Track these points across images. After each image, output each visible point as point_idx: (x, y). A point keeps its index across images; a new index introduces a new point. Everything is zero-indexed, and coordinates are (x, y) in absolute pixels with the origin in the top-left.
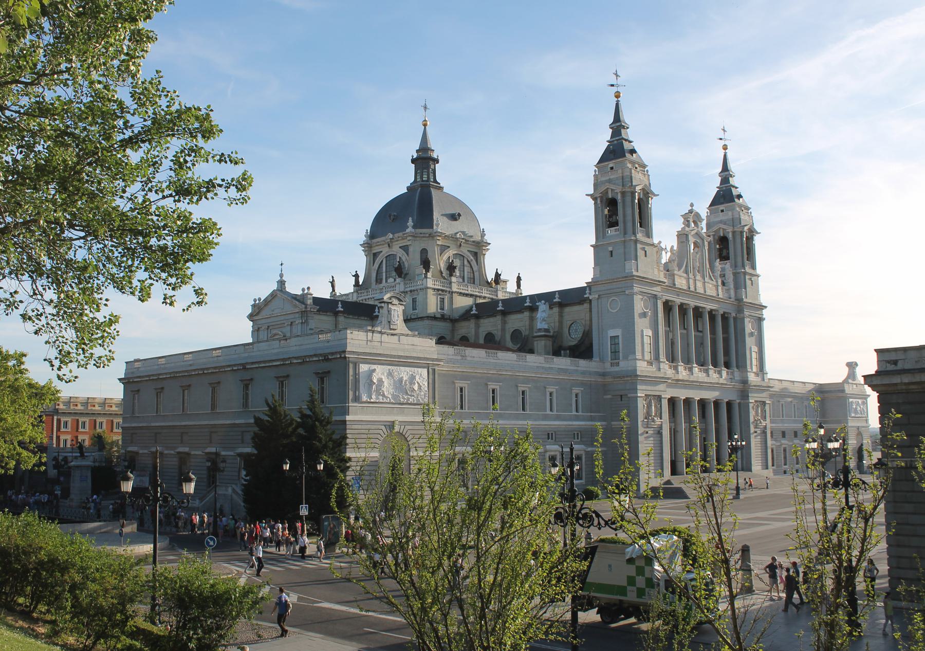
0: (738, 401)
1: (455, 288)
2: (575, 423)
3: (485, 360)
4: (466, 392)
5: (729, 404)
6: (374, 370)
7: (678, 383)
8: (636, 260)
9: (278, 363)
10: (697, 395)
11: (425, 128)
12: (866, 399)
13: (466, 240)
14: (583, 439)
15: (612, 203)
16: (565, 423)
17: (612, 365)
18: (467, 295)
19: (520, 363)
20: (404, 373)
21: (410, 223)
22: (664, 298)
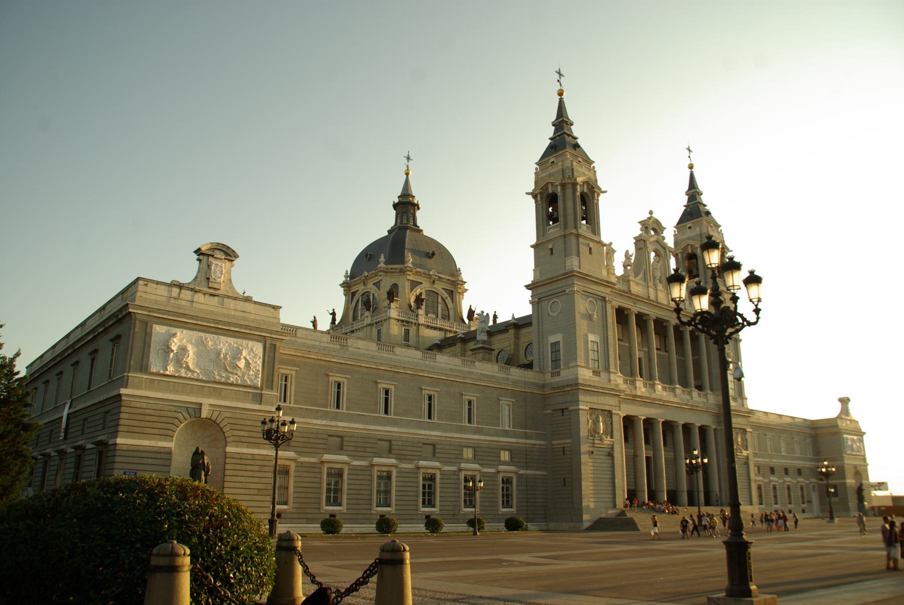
0: (713, 427)
1: (422, 320)
2: (502, 439)
3: (376, 354)
4: (345, 390)
5: (703, 430)
6: (174, 335)
7: (634, 399)
8: (579, 256)
9: (90, 337)
10: (660, 415)
11: (407, 177)
12: (862, 436)
13: (439, 277)
14: (513, 460)
15: (552, 200)
16: (488, 438)
17: (553, 375)
18: (435, 328)
19: (427, 363)
20: (225, 344)
21: (382, 259)
22: (616, 304)
